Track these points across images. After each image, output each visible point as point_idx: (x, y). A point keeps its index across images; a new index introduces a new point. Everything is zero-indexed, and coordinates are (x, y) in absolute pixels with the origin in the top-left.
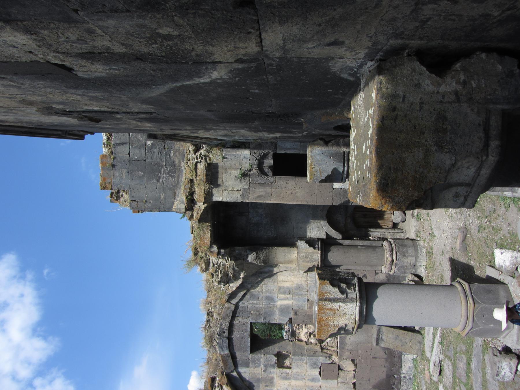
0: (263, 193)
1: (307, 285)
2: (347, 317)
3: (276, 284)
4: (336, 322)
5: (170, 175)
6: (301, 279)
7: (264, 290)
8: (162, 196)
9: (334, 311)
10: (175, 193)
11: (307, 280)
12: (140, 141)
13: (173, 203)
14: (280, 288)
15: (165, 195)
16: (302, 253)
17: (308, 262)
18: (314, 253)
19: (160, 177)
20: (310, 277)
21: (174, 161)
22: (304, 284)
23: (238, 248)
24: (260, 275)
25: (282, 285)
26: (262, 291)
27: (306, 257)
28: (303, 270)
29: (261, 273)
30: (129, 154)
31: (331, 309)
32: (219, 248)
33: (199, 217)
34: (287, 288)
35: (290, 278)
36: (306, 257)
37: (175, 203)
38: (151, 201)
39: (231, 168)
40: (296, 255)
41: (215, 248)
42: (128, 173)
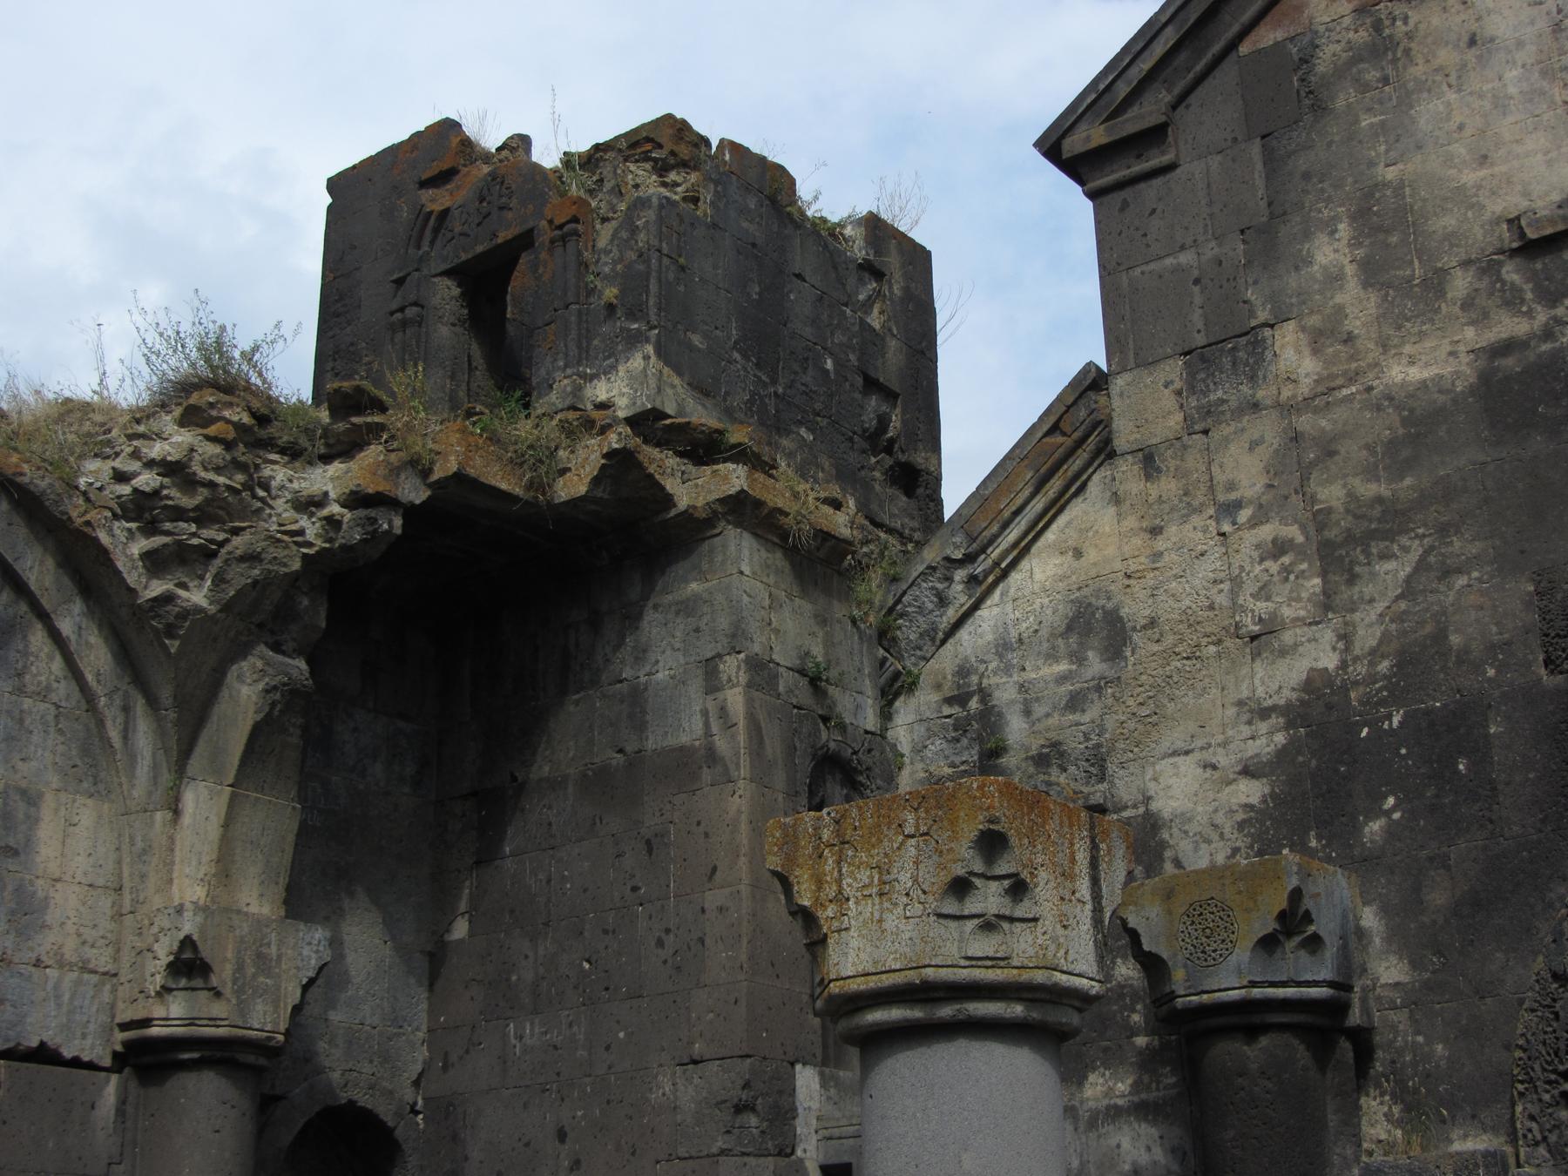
0: (769, 751)
1: (38, 963)
2: (1060, 931)
3: (55, 780)
4: (1043, 875)
5: (751, 402)
6: (70, 928)
7: (27, 703)
8: (696, 339)
9: (1068, 876)
10: (707, 394)
11: (62, 964)
12: (832, 334)
13: (680, 374)
14: (31, 799)
15: (699, 350)
16: (281, 943)
17: (240, 968)
18: (276, 1003)
19: (745, 357)
20: (78, 983)
21: (788, 433)
22: (45, 943)
23: (323, 614)
24: (118, 702)
25: (46, 812)
26: (20, 691)
27: (259, 956)
28: (203, 930)
29: (126, 709)
30: (798, 276)
31: (1073, 861)
32: (411, 513)
33: (641, 457)
34: (28, 840)
35: (80, 864)
36: (259, 956)
37: (677, 381)
38: (682, 288)
39: (829, 643)
40: (254, 909)
41: (413, 492)
42: (754, 245)
